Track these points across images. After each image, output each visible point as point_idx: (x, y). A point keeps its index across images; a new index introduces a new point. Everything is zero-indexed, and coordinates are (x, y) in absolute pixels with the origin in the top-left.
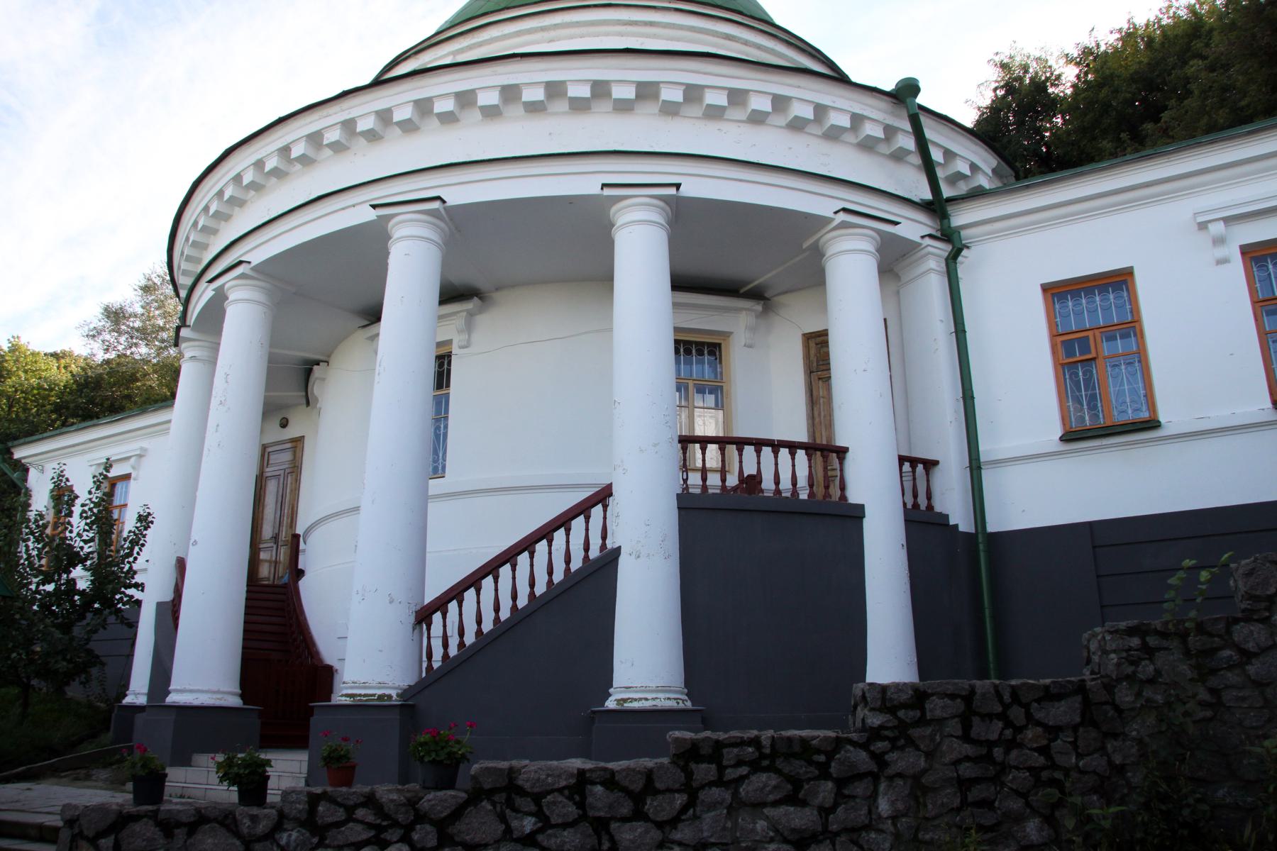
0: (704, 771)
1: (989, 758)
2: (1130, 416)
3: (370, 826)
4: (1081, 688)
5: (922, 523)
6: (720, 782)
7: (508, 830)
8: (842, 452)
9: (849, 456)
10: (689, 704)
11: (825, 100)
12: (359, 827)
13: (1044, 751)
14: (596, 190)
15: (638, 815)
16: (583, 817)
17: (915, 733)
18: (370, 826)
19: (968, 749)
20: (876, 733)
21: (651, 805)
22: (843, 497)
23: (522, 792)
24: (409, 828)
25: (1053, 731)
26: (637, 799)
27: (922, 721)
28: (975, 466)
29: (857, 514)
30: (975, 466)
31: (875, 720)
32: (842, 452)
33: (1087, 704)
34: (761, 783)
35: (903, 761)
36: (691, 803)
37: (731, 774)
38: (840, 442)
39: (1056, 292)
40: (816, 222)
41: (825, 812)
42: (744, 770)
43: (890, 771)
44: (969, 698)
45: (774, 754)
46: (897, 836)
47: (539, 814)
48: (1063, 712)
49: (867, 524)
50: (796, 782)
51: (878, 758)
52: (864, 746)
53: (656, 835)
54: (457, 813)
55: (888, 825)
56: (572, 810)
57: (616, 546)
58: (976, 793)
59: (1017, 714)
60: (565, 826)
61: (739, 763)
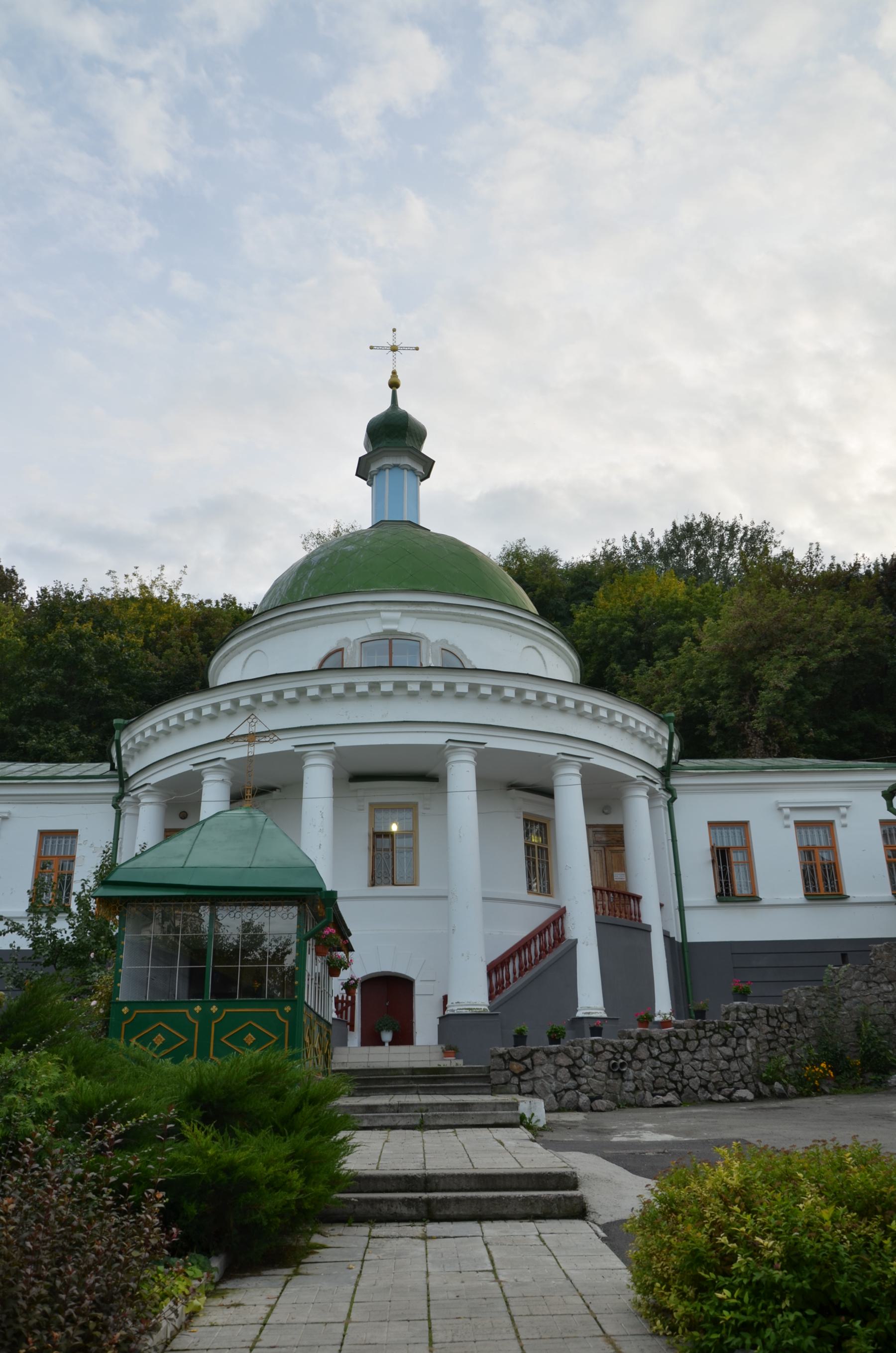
0: (701, 1032)
1: (774, 1032)
2: (745, 892)
3: (612, 1053)
4: (797, 1010)
5: (666, 935)
6: (705, 1037)
7: (651, 1054)
8: (638, 899)
9: (642, 902)
10: (605, 1016)
11: (640, 719)
12: (608, 1053)
13: (788, 1031)
14: (554, 754)
15: (685, 1049)
16: (671, 1049)
17: (756, 1021)
18: (612, 1053)
19: (769, 1029)
20: (744, 1021)
21: (688, 1045)
22: (640, 921)
23: (654, 1040)
24: (622, 1053)
25: (790, 1024)
26: (685, 1042)
27: (756, 1018)
28: (681, 909)
29: (647, 930)
30: (681, 909)
31: (744, 1016)
32: (638, 899)
33: (798, 1016)
34: (717, 1038)
35: (753, 1032)
36: (699, 1045)
37: (709, 1034)
38: (638, 893)
39: (712, 825)
40: (626, 780)
41: (734, 1049)
42: (711, 1033)
43: (750, 1035)
44: (768, 1011)
45: (719, 1028)
46: (753, 1059)
47: (659, 1048)
48: (792, 1017)
49: (652, 934)
50: (726, 1039)
51: (746, 1030)
52: (742, 1026)
53: (690, 1056)
54: (635, 1048)
55: (750, 1055)
56: (667, 1046)
57: (574, 938)
58: (773, 1045)
59: (780, 1016)
60: (666, 1052)
61: (710, 1030)
